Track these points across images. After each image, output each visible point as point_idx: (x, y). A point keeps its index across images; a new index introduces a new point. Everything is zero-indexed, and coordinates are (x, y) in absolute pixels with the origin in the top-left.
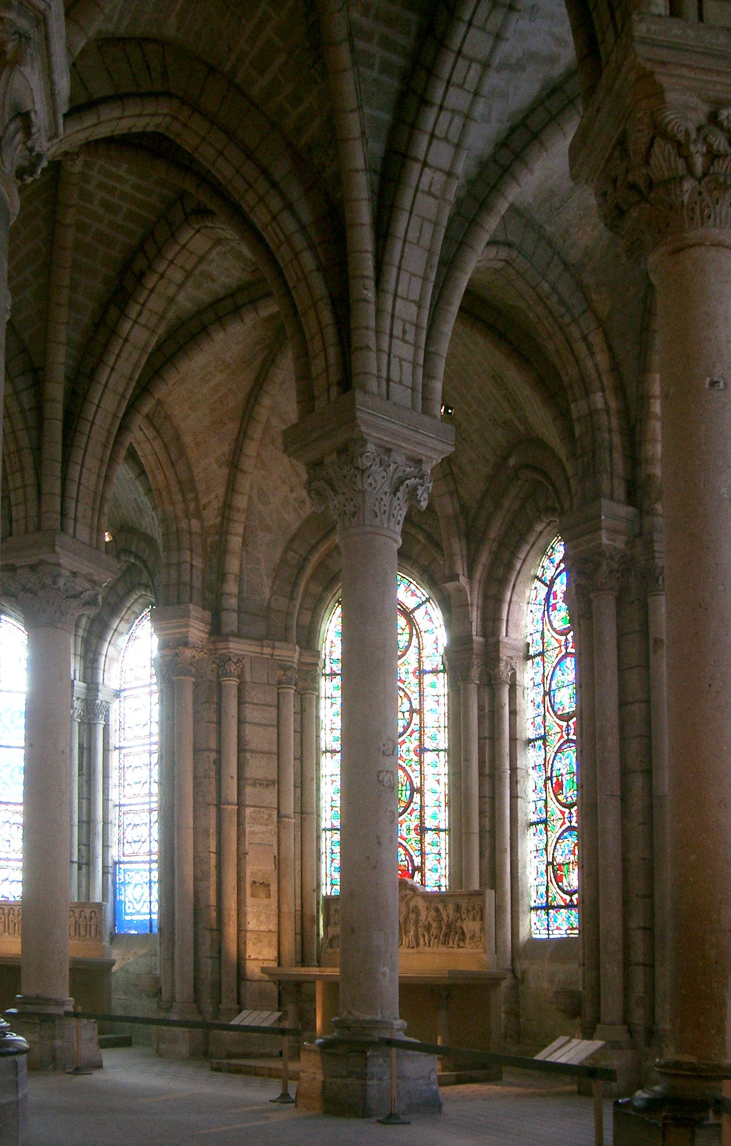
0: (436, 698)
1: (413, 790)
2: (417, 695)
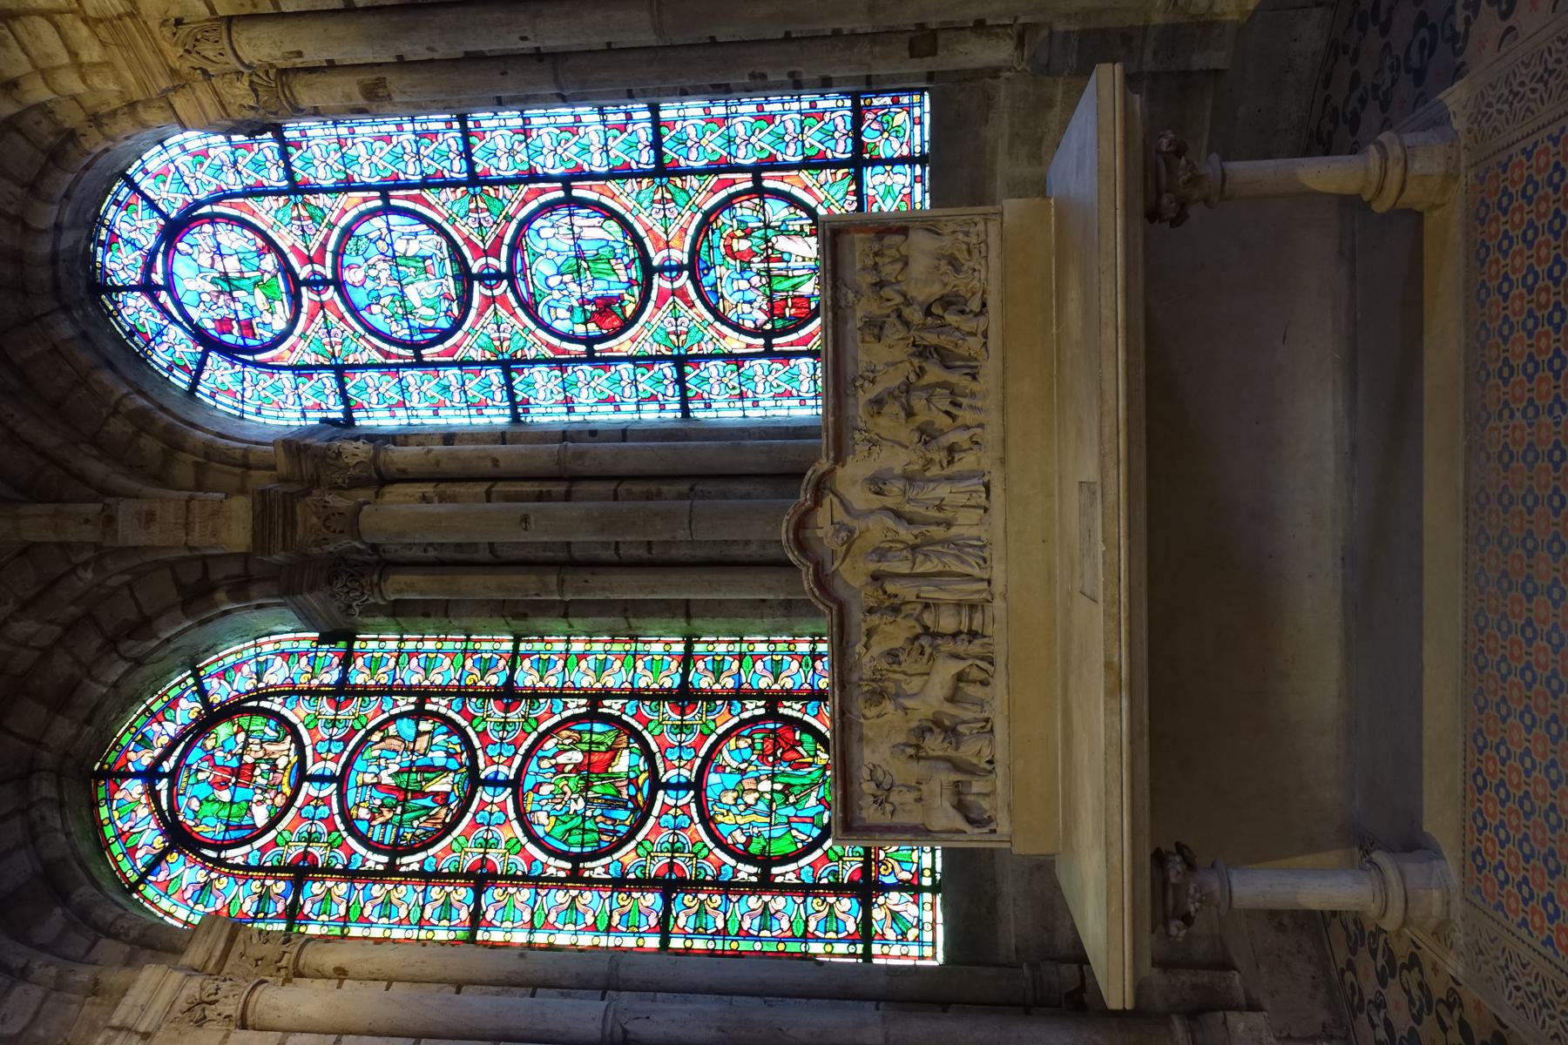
0: (404, 658)
1: (593, 716)
2: (388, 703)
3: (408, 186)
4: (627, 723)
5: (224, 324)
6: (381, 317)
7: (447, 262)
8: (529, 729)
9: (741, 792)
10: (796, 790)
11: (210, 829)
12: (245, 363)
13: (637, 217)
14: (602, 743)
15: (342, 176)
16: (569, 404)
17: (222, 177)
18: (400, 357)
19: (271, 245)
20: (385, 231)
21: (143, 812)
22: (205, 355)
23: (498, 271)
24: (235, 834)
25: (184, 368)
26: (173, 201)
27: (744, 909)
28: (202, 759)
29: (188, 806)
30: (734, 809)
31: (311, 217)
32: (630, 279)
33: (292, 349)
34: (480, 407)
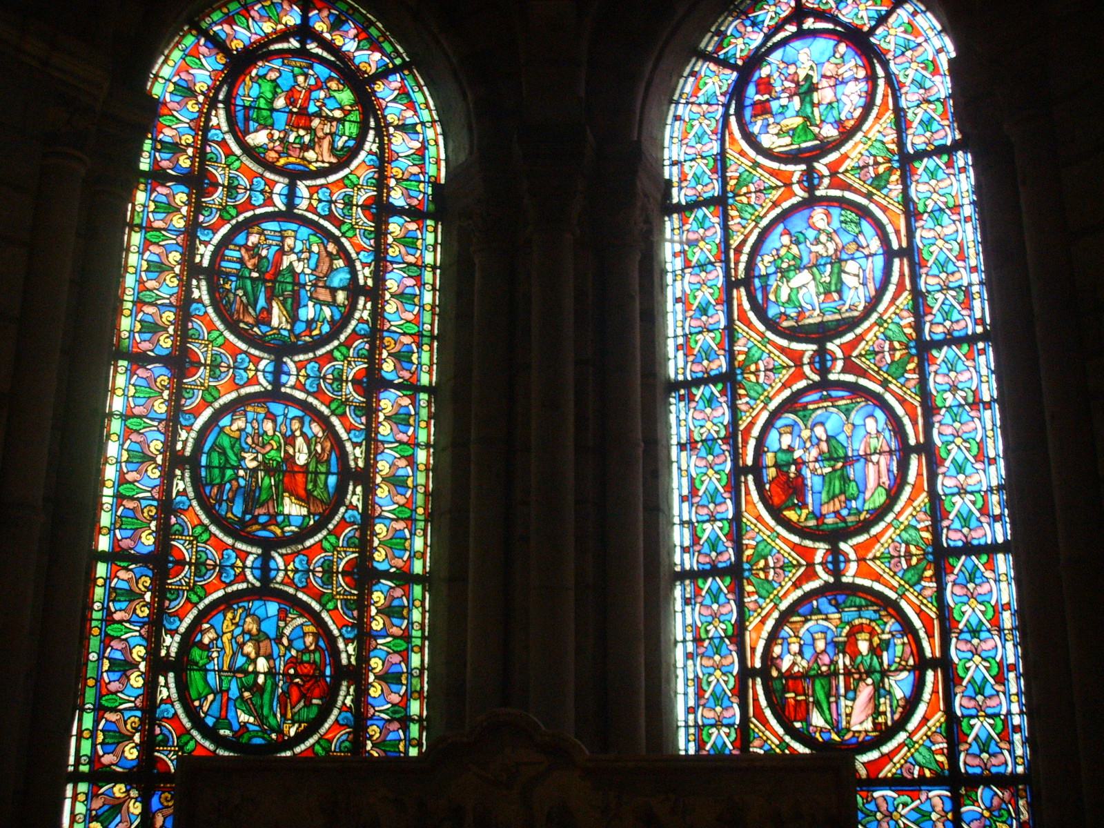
0: (414, 271)
2: (365, 257)
3: (914, 277)
4: (336, 512)
5: (765, 86)
6: (778, 245)
7: (837, 317)
8: (333, 406)
9: (258, 638)
10: (257, 700)
11: (249, 91)
12: (726, 106)
13: (890, 525)
14: (315, 485)
15: (921, 209)
16: (690, 445)
17: (914, 88)
18: (737, 263)
19: (847, 134)
20: (866, 252)
21: (268, 27)
22: (734, 67)
23: (829, 371)
24: (240, 115)
25: (720, 46)
26: (888, 38)
27: (132, 642)
28: (317, 79)
29: (272, 69)
30: (238, 631)
31: (878, 176)
32: (823, 516)
33: (742, 153)
34: (685, 347)
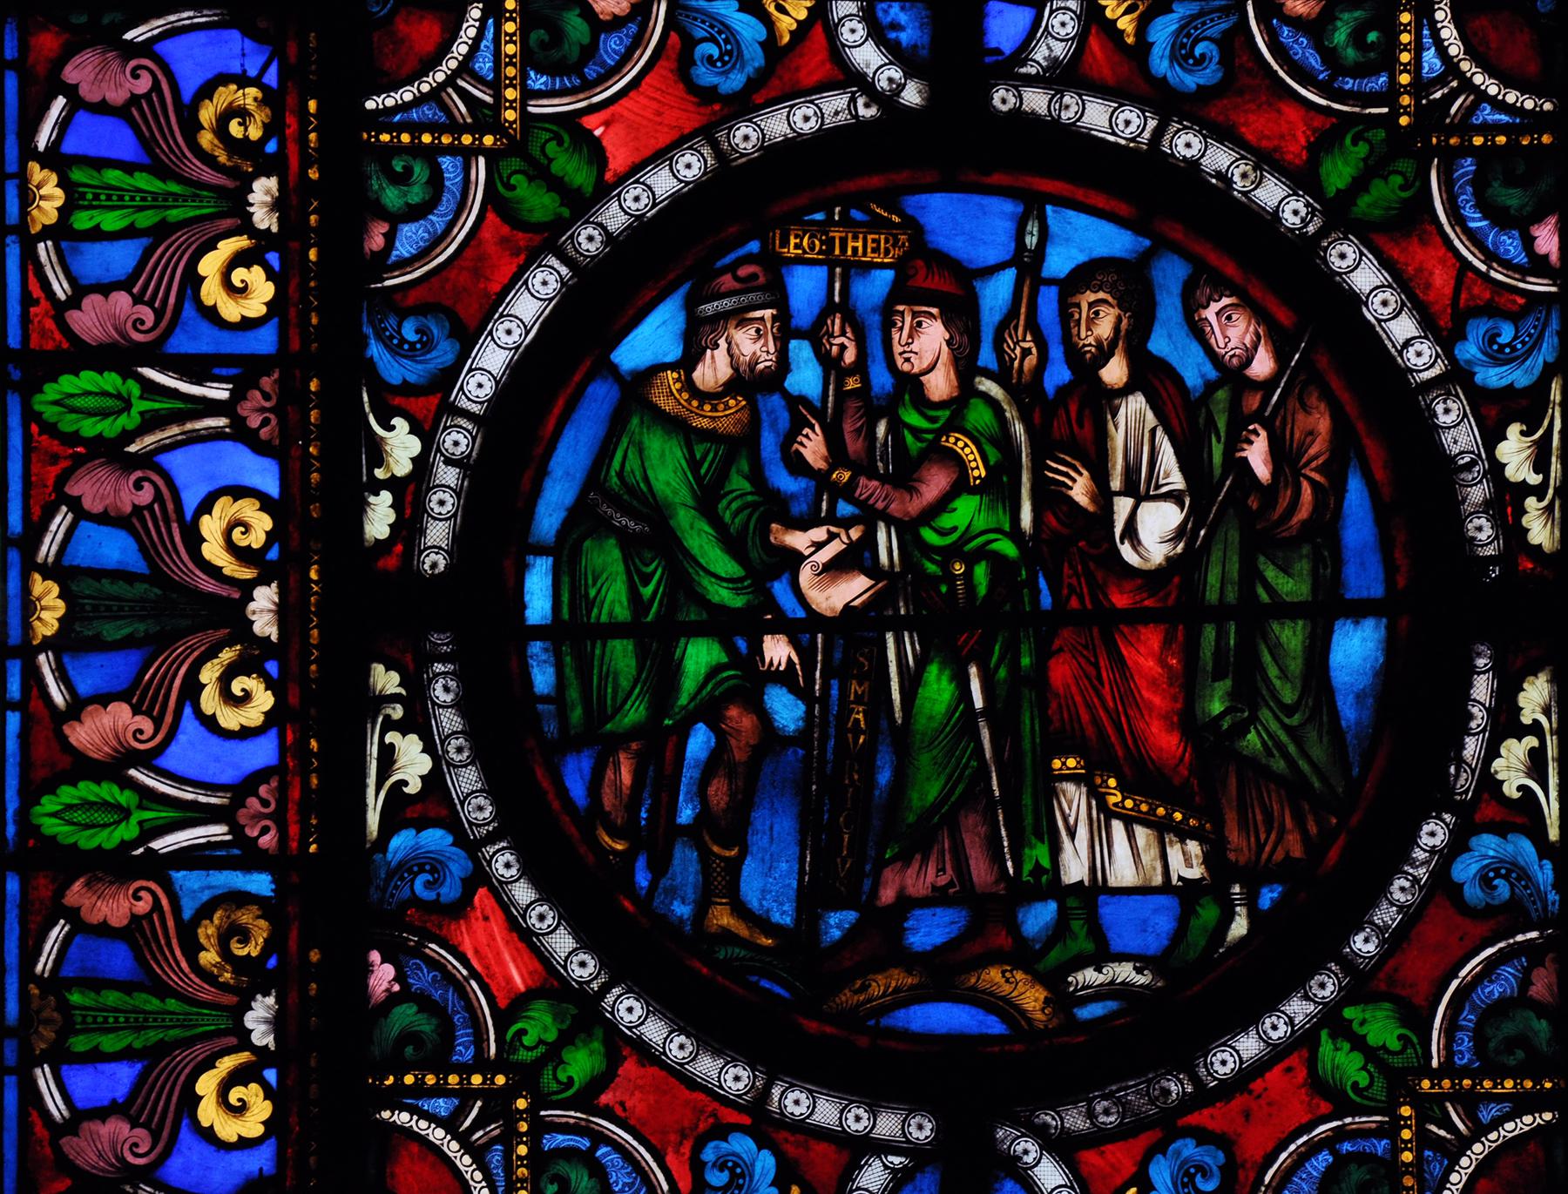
4: (1399, 858)
8: (1338, 173)
14: (1250, 697)
